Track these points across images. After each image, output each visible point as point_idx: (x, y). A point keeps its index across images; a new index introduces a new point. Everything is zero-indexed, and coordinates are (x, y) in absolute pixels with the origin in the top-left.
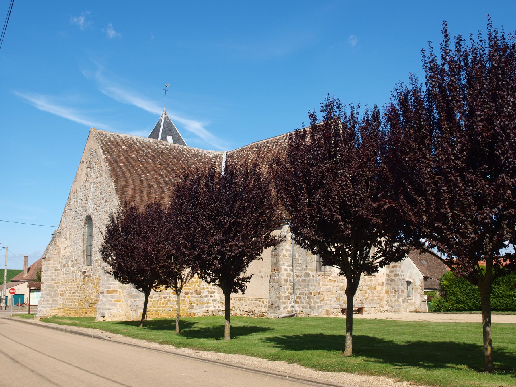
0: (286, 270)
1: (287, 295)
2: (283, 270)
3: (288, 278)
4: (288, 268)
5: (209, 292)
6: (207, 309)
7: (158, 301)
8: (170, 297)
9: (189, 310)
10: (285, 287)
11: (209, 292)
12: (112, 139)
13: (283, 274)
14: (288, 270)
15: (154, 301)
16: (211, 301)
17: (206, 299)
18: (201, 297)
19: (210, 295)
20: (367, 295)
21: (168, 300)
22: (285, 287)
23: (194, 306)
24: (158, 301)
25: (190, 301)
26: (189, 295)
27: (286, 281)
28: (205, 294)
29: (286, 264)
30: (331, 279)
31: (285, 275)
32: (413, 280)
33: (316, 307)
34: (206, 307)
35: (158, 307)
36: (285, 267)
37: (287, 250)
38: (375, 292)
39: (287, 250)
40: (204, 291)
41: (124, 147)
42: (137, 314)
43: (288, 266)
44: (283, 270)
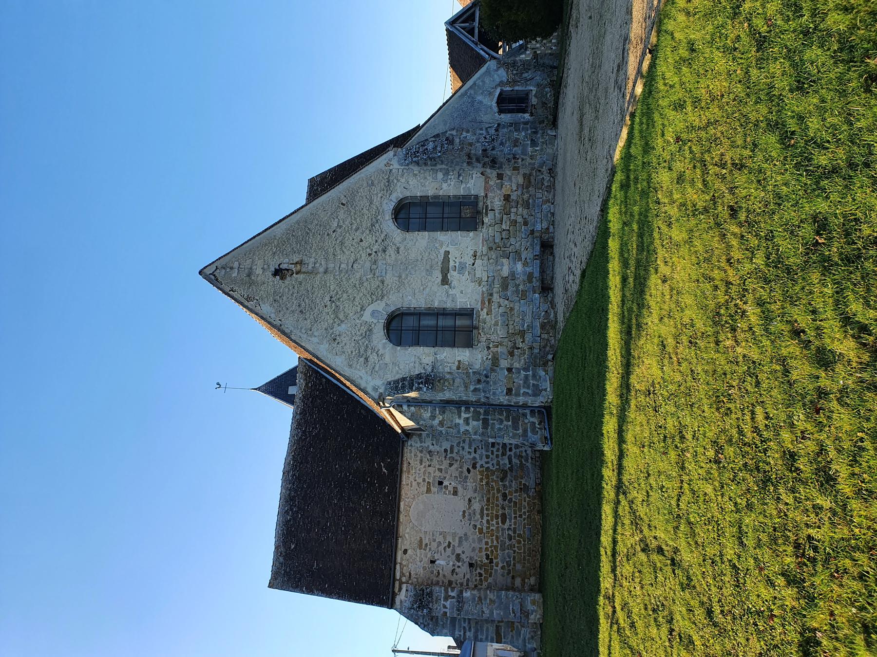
0: (467, 421)
1: (510, 423)
2: (467, 428)
3: (482, 417)
4: (464, 415)
5: (503, 454)
6: (530, 460)
7: (515, 551)
8: (509, 529)
9: (531, 494)
10: (497, 426)
11: (503, 454)
12: (281, 559)
13: (473, 427)
14: (467, 416)
15: (514, 559)
16: (518, 450)
17: (514, 460)
18: (511, 469)
19: (508, 453)
20: (520, 219)
21: (515, 532)
22: (497, 426)
23: (524, 484)
24: (515, 551)
25: (516, 491)
26: (507, 492)
27: (485, 423)
28: (507, 461)
29: (457, 421)
30: (485, 310)
31: (475, 423)
32: (496, 87)
33: (535, 383)
34: (527, 460)
35: (524, 552)
36: (461, 422)
37: (433, 417)
38: (513, 197)
39: (433, 417)
40: (501, 462)
41: (293, 546)
42: (533, 611)
43: (460, 417)
44: (467, 428)
